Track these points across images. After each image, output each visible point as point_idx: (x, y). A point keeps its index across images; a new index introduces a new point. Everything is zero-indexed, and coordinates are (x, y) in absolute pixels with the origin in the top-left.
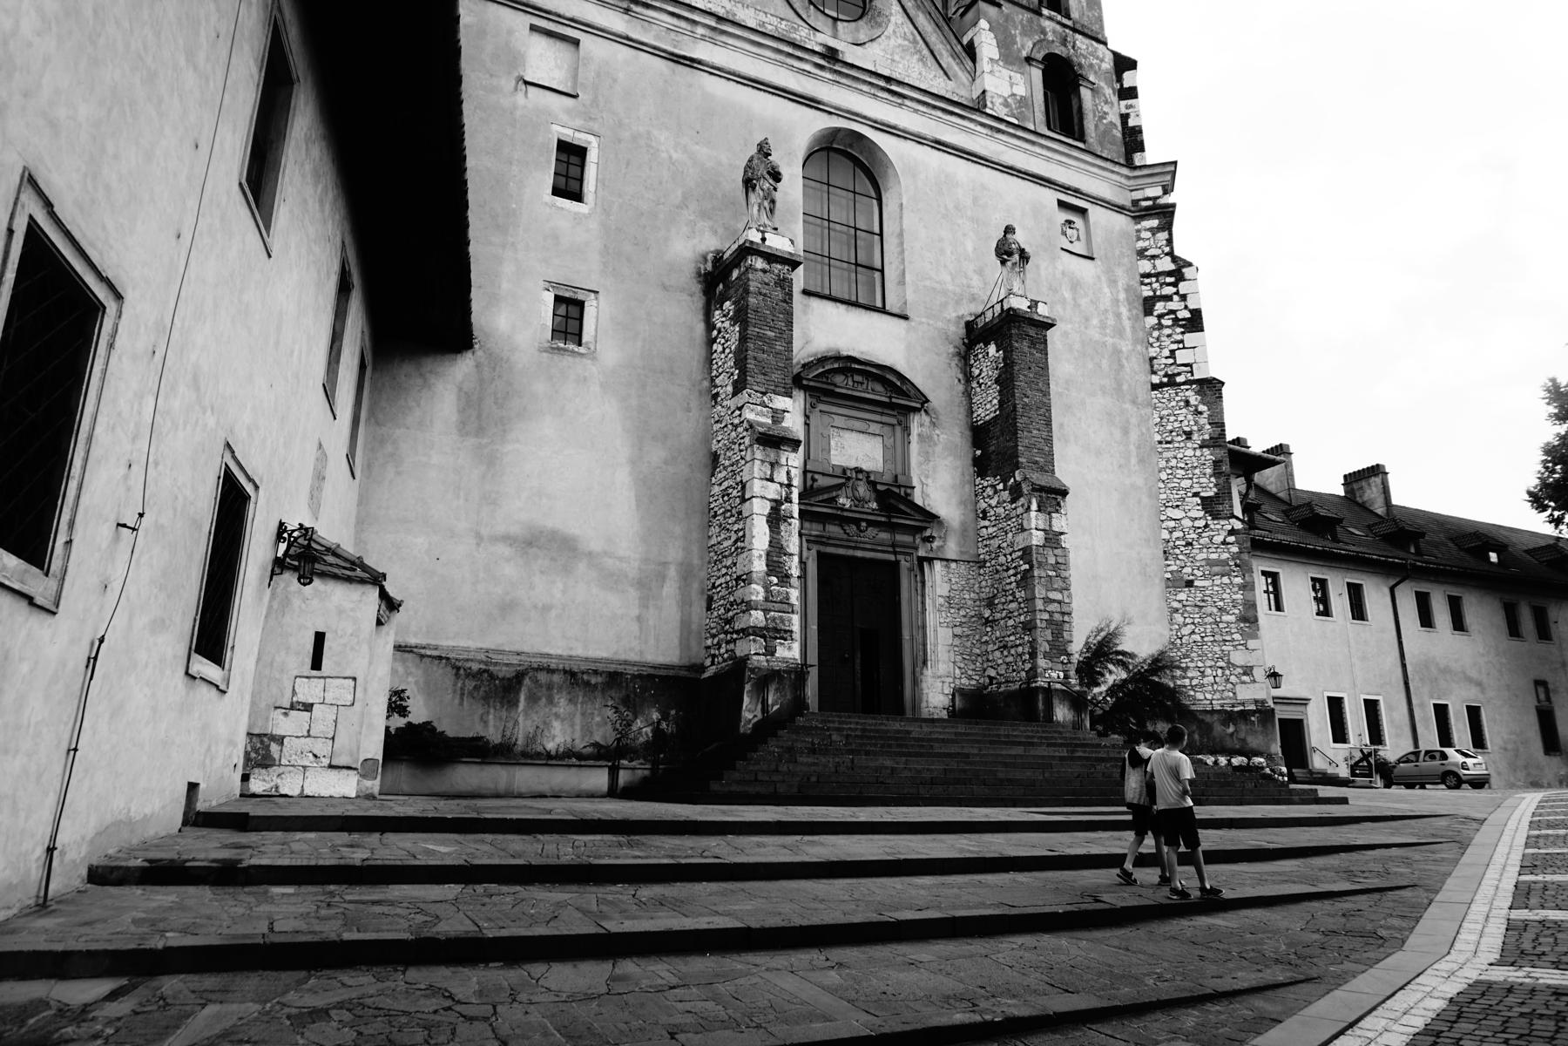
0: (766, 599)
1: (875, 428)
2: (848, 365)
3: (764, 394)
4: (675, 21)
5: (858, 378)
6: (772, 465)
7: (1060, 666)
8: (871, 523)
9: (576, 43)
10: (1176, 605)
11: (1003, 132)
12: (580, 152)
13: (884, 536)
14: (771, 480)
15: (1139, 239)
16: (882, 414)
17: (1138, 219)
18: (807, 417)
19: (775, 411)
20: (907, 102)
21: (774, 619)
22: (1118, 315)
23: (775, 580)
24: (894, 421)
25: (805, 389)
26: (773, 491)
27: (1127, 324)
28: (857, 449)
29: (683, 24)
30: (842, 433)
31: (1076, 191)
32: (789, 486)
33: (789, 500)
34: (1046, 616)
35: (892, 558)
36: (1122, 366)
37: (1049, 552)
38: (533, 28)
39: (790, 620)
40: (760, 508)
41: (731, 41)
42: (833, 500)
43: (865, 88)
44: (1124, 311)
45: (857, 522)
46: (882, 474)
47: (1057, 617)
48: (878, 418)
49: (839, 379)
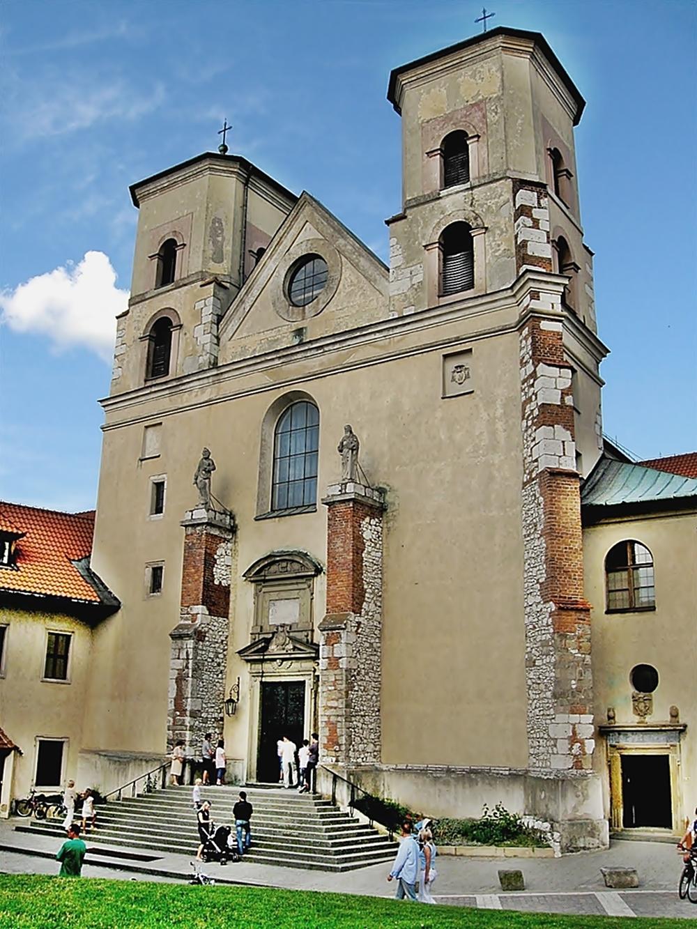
0: (174, 724)
1: (295, 594)
2: (271, 560)
3: (188, 607)
4: (201, 382)
5: (284, 564)
6: (179, 649)
7: (334, 753)
8: (283, 660)
9: (161, 423)
10: (529, 682)
11: (396, 327)
12: (163, 483)
13: (296, 665)
14: (179, 658)
15: (521, 349)
16: (297, 583)
17: (520, 329)
18: (255, 598)
19: (193, 615)
20: (326, 349)
21: (177, 734)
22: (493, 433)
23: (178, 713)
24: (306, 586)
25: (252, 582)
26: (179, 664)
27: (501, 436)
28: (285, 612)
29: (205, 381)
30: (276, 603)
31: (457, 339)
32: (188, 659)
33: (187, 667)
34: (326, 719)
35: (301, 679)
36: (491, 478)
37: (332, 672)
38: (147, 427)
39: (185, 734)
40: (175, 674)
41: (226, 376)
42: (265, 649)
43: (299, 356)
44: (500, 425)
45: (275, 660)
46: (297, 624)
47: (333, 719)
48: (295, 587)
49: (274, 568)
